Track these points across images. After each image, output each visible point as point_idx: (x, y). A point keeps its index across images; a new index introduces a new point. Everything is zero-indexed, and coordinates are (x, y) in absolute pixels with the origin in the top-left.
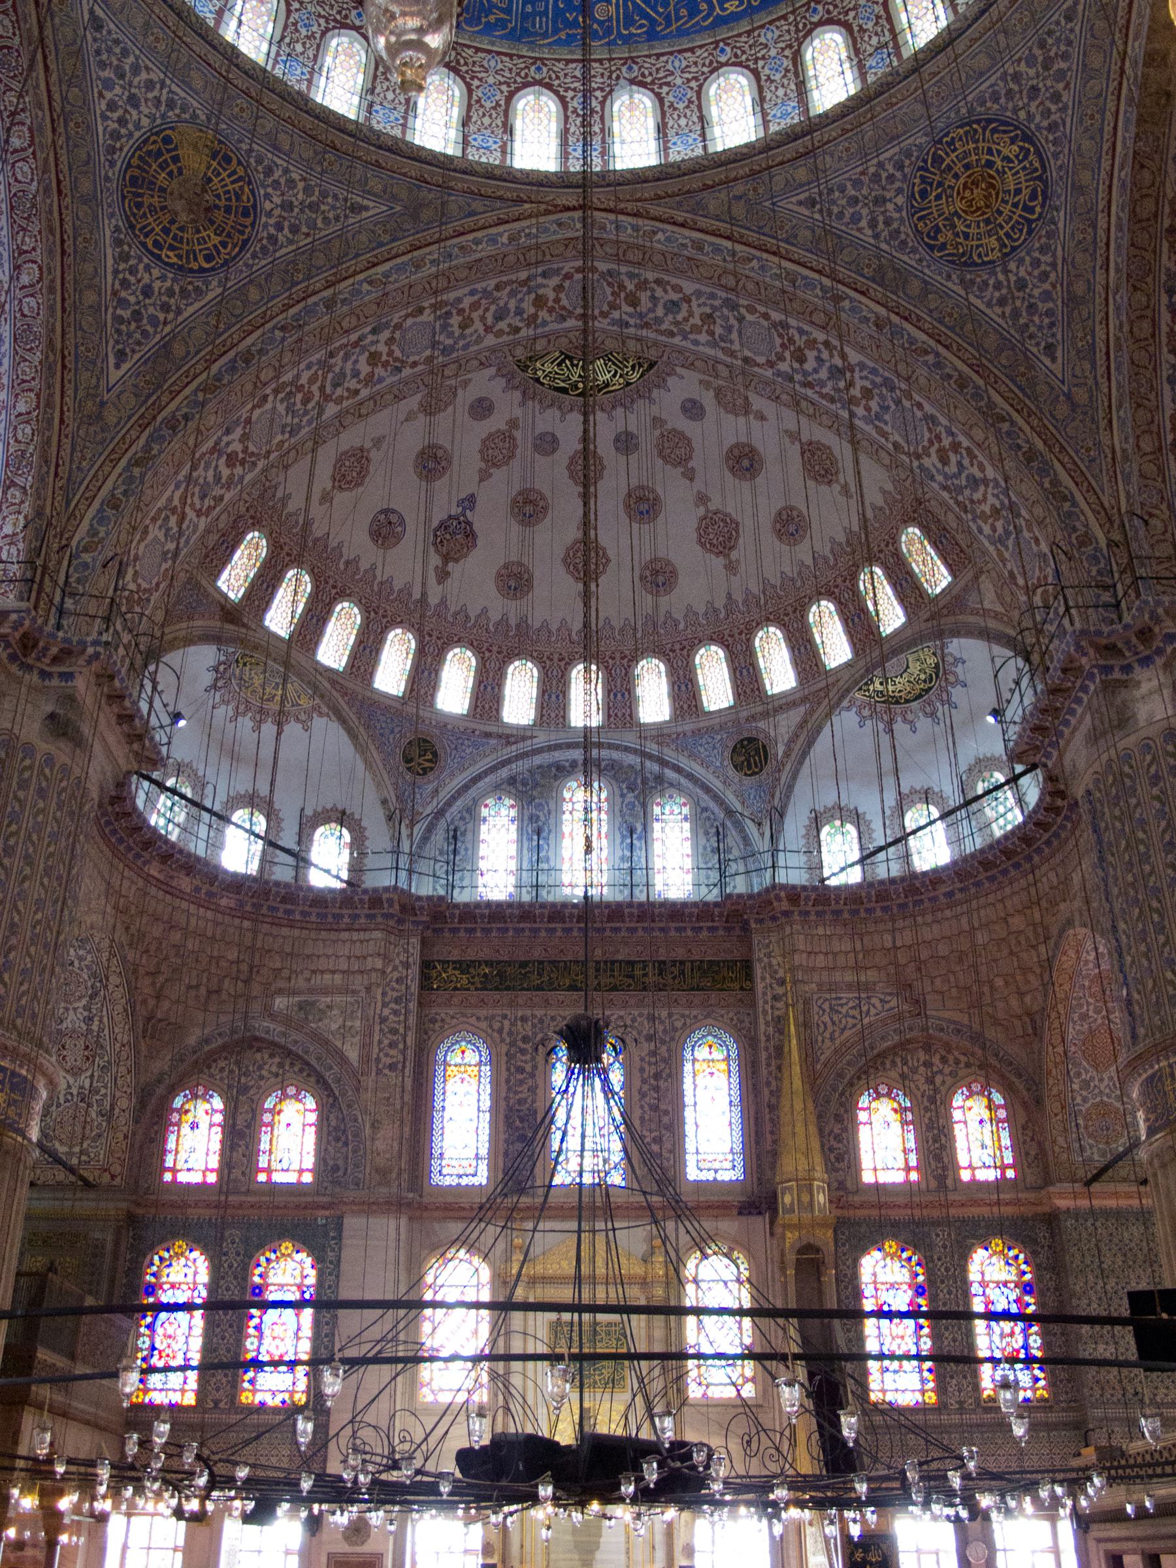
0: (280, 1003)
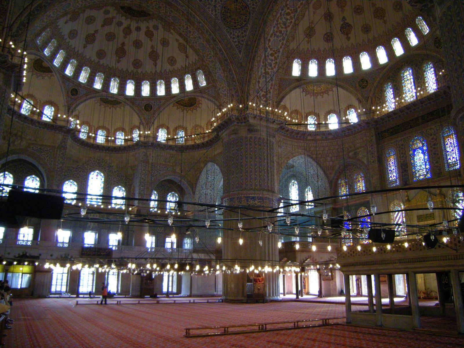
0: (350, 154)
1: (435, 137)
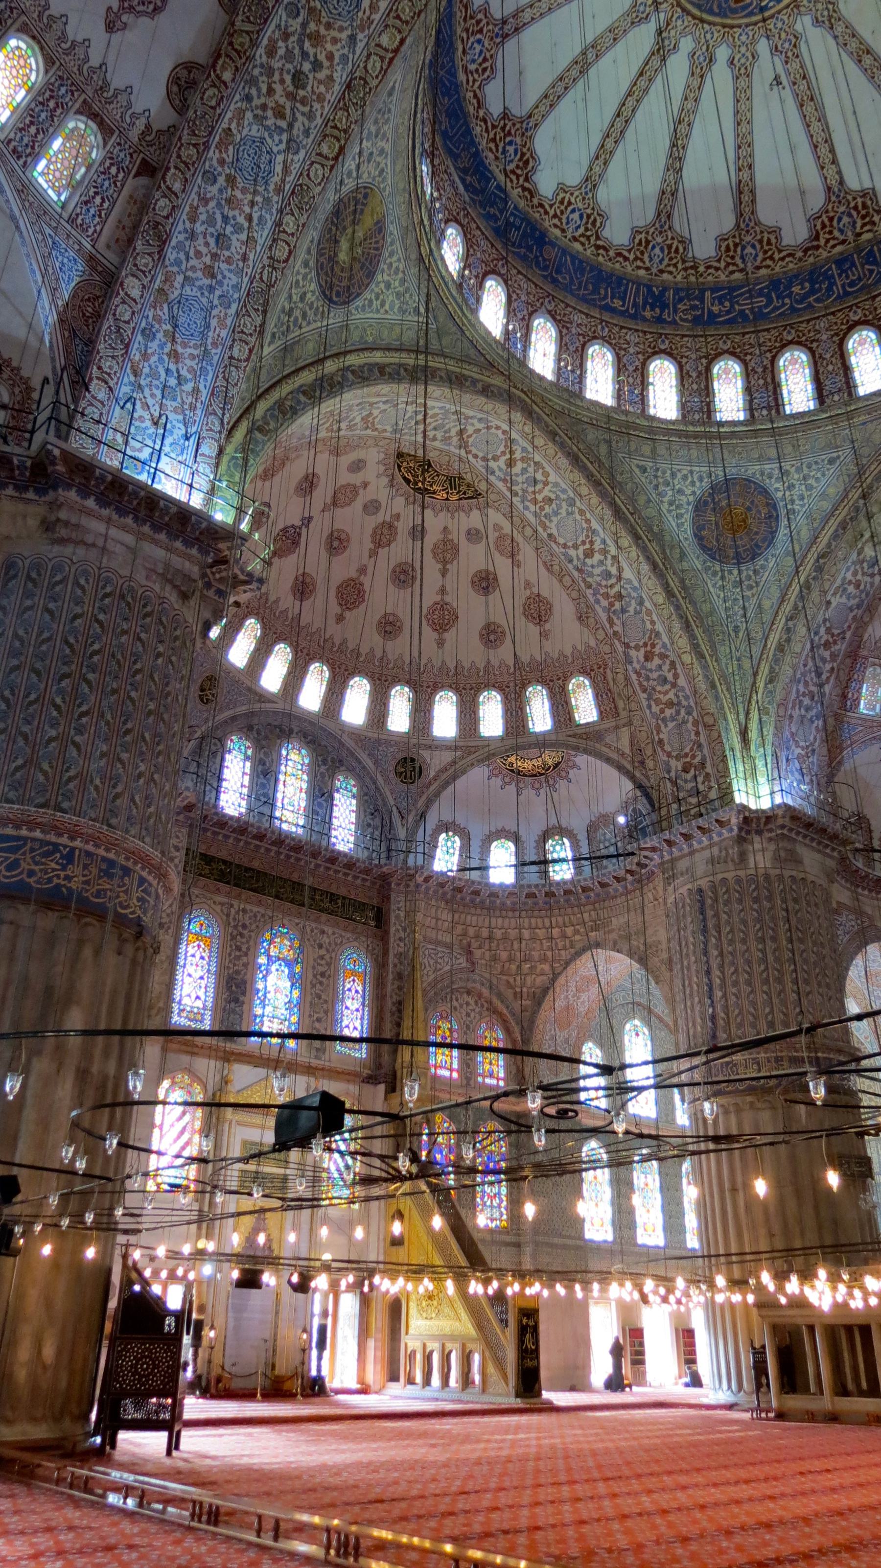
1: (327, 957)
